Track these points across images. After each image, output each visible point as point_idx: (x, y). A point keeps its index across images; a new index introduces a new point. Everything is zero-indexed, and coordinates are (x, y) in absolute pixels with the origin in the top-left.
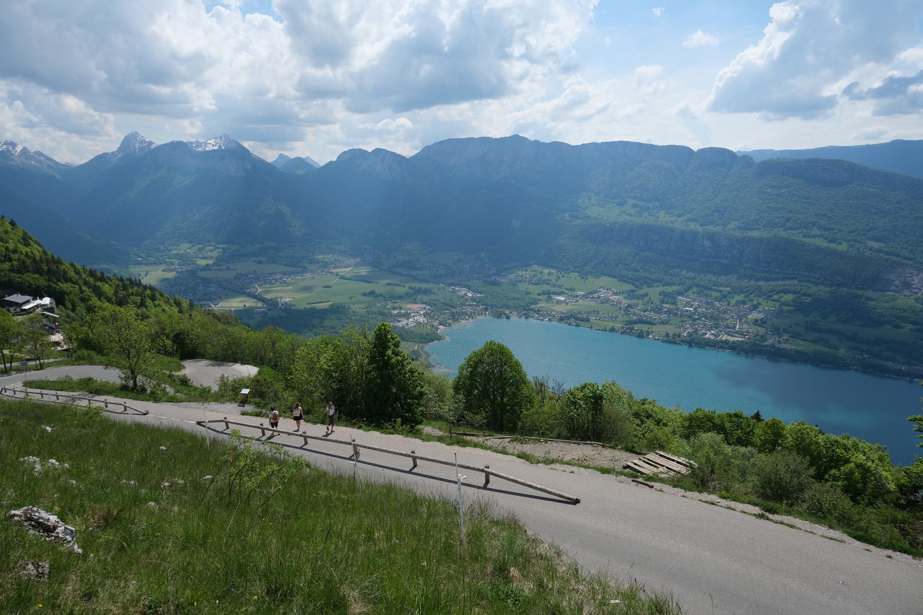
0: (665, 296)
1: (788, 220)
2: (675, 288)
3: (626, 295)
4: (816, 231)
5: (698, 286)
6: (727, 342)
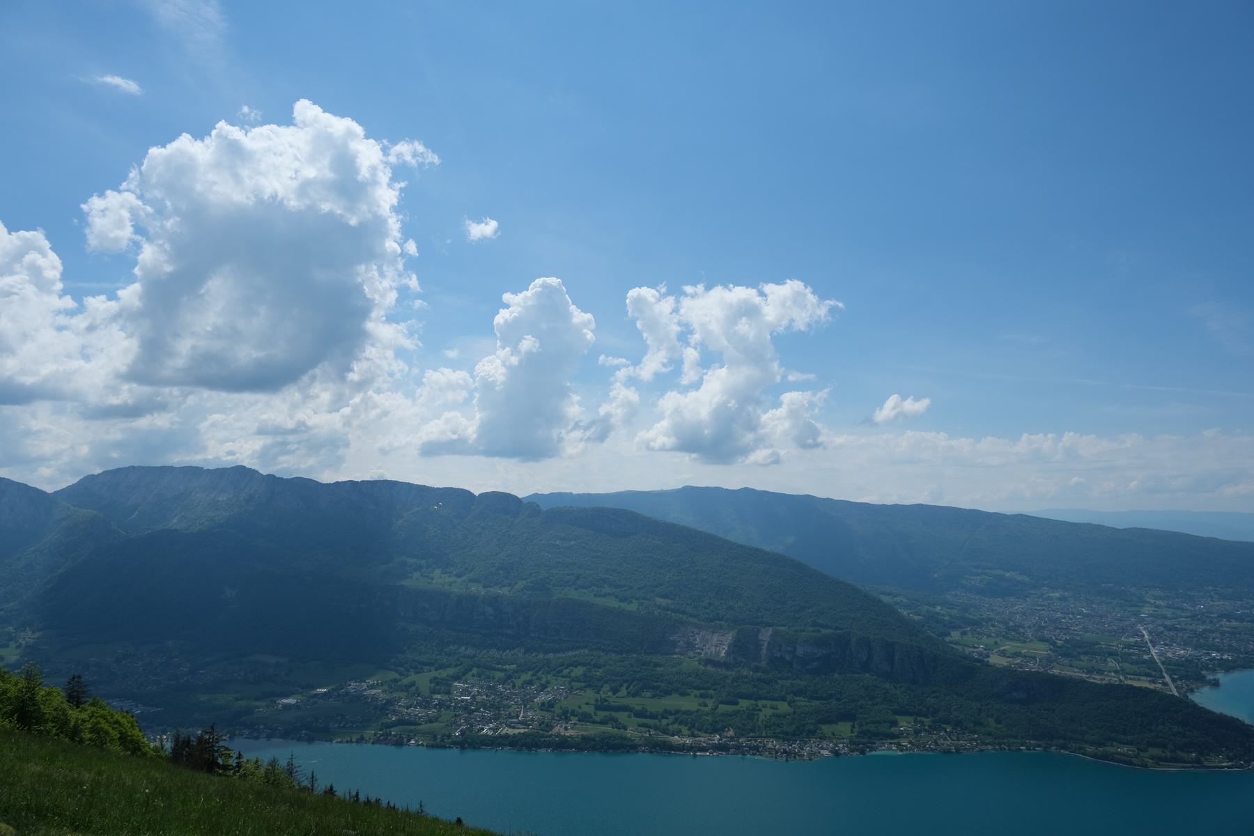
0: (437, 684)
1: (578, 577)
2: (451, 671)
3: (386, 687)
4: (607, 589)
5: (478, 666)
6: (507, 736)
